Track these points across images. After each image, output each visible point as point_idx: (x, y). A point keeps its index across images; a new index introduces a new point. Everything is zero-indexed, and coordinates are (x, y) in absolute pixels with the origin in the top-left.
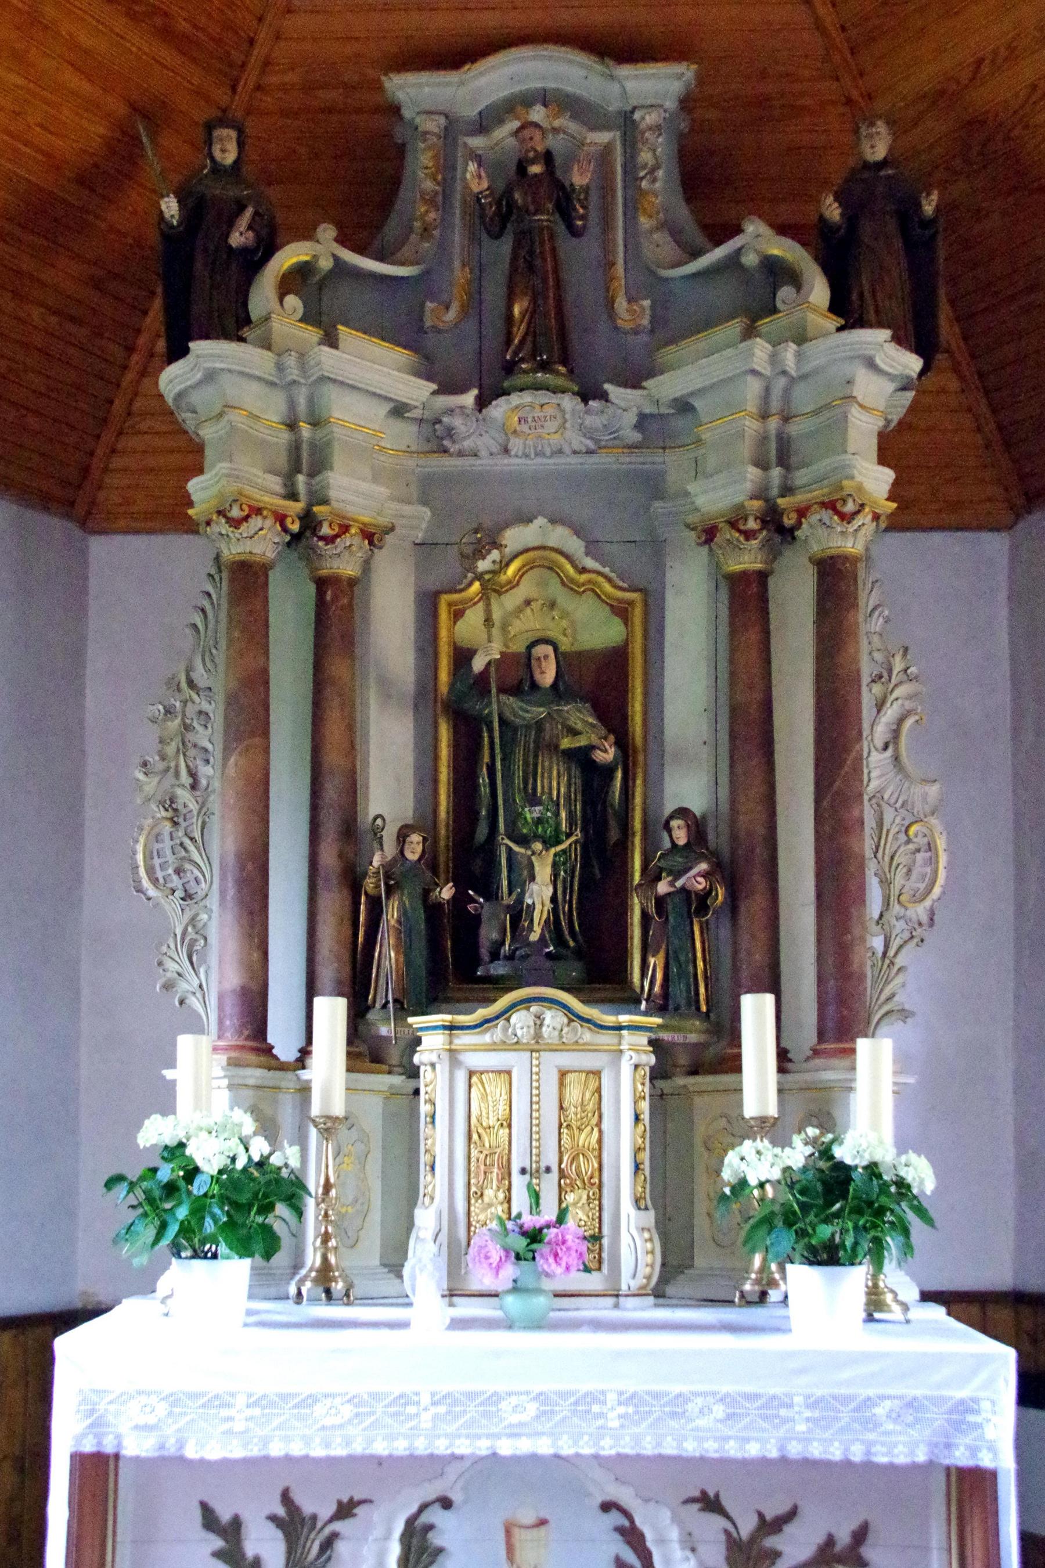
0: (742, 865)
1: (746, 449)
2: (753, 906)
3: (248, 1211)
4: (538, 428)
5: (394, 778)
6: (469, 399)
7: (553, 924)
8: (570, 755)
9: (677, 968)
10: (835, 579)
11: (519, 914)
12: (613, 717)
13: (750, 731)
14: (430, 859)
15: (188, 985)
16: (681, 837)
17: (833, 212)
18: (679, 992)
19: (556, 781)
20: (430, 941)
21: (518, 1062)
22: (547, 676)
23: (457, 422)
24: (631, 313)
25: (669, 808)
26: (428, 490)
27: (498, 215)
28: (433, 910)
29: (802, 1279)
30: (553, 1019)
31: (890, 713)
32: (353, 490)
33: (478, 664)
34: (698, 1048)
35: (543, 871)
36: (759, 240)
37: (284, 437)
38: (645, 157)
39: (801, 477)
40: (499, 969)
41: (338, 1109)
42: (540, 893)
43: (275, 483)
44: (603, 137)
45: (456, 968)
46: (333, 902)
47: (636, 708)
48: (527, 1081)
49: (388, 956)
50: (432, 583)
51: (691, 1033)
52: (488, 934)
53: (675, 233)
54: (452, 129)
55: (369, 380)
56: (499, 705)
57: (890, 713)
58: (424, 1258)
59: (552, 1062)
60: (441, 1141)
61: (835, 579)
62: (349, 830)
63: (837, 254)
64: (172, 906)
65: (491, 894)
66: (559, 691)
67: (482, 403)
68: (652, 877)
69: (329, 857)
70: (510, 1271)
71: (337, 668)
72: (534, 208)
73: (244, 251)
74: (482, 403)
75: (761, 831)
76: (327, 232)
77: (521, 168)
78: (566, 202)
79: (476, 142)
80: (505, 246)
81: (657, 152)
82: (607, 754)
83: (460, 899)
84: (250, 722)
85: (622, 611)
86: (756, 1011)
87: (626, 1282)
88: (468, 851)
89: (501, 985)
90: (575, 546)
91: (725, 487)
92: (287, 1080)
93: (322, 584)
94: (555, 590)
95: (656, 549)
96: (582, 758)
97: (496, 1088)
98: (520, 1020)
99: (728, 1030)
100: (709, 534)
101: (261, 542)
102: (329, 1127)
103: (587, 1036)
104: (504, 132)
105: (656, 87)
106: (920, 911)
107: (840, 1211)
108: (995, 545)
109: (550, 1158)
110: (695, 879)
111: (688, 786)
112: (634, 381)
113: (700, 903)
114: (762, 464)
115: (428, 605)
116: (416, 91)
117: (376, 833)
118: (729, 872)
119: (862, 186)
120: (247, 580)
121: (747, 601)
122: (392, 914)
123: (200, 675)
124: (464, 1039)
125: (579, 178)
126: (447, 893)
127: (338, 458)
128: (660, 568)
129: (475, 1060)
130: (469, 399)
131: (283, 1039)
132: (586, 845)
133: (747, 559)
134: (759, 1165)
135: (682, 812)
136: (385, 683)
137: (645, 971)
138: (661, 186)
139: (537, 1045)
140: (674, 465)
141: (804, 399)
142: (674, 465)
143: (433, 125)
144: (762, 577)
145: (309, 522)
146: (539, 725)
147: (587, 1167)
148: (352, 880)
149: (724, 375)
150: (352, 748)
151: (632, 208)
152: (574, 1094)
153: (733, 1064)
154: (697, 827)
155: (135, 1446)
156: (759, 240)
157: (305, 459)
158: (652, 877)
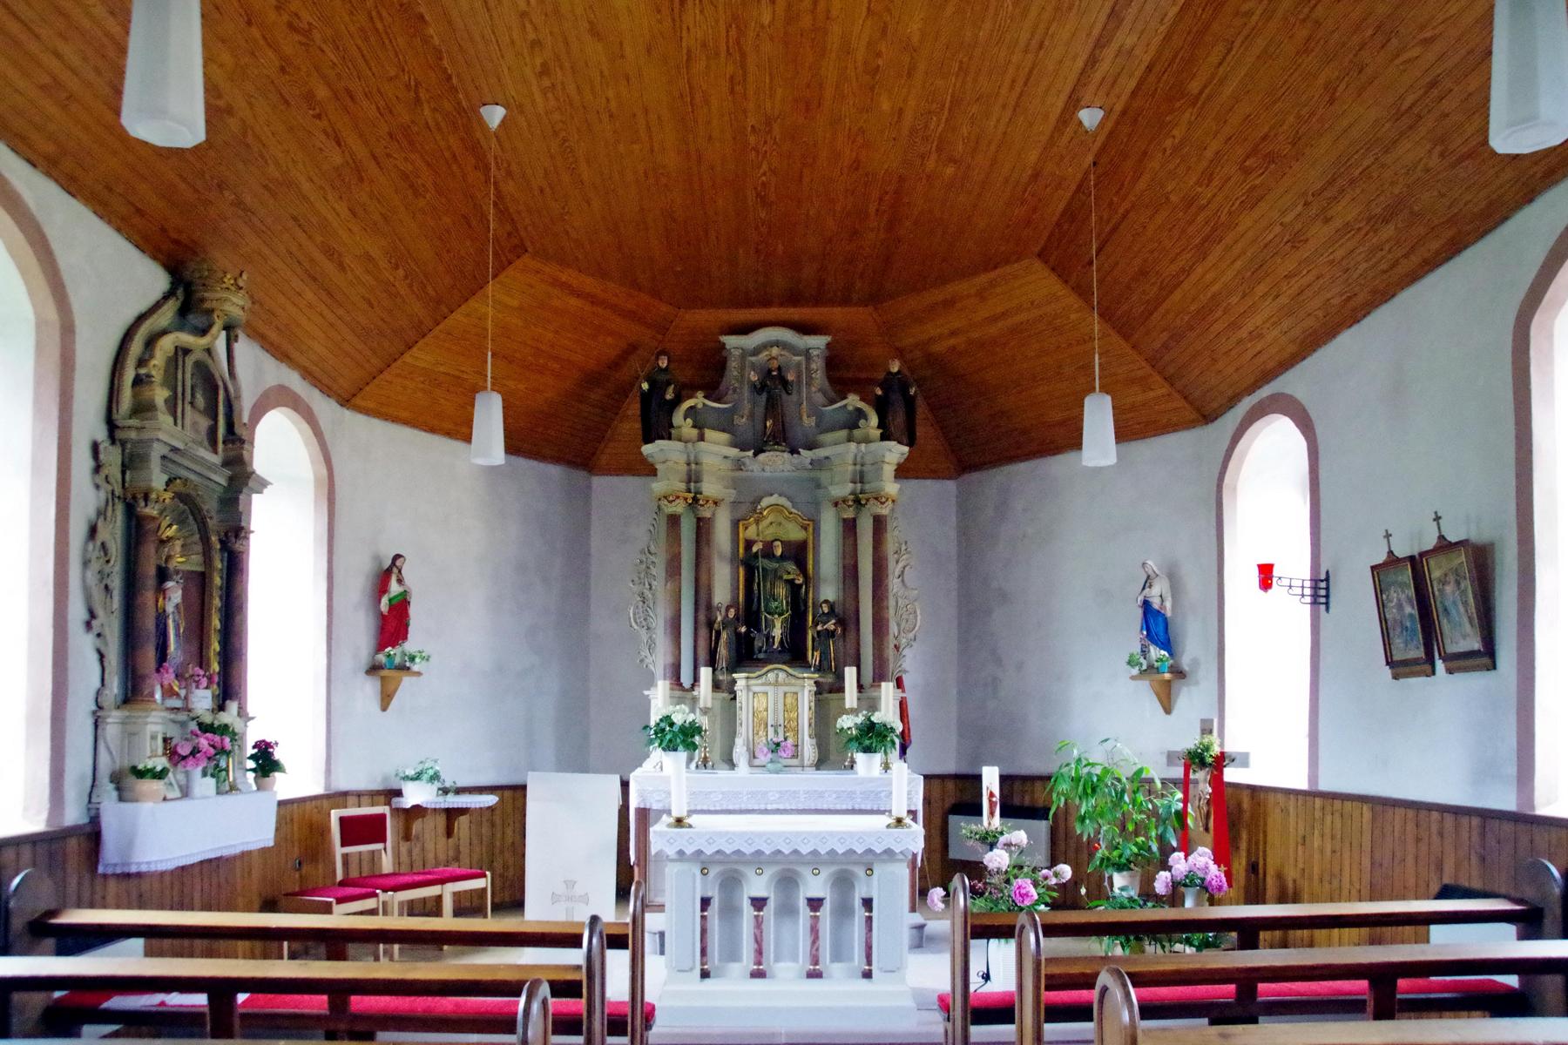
0: (847, 619)
1: (849, 477)
2: (851, 636)
3: (682, 737)
4: (776, 462)
5: (723, 591)
6: (751, 453)
7: (781, 642)
8: (787, 581)
9: (824, 655)
10: (879, 524)
11: (769, 638)
12: (802, 566)
13: (850, 574)
14: (737, 617)
15: (649, 660)
16: (826, 610)
17: (879, 392)
18: (825, 664)
19: (782, 591)
20: (739, 646)
21: (770, 690)
22: (778, 552)
23: (747, 461)
24: (809, 422)
25: (822, 599)
26: (735, 484)
27: (759, 389)
28: (738, 635)
29: (860, 757)
30: (782, 675)
31: (901, 565)
32: (710, 488)
33: (755, 549)
34: (831, 684)
35: (778, 624)
36: (853, 401)
37: (685, 468)
38: (814, 366)
39: (867, 487)
40: (761, 656)
41: (709, 705)
42: (777, 632)
43: (683, 486)
44: (797, 358)
45: (746, 656)
46: (703, 632)
47: (810, 562)
48: (773, 696)
49: (723, 651)
50: (738, 516)
51: (829, 679)
52: (758, 644)
53: (825, 394)
54: (745, 353)
55: (716, 450)
56: (762, 562)
57: (901, 565)
58: (740, 753)
59: (782, 689)
60: (744, 715)
61: (879, 524)
62: (709, 607)
63: (882, 407)
64: (644, 631)
65: (759, 630)
66: (783, 557)
67: (755, 455)
68: (815, 624)
69: (702, 617)
70: (770, 755)
71: (705, 550)
72: (773, 385)
73: (671, 401)
74: (755, 455)
75: (853, 608)
76: (700, 394)
77: (770, 371)
78: (785, 383)
79: (753, 359)
80: (764, 396)
81: (818, 365)
82: (800, 581)
83: (748, 632)
84: (674, 569)
85: (805, 528)
86: (850, 673)
87: (806, 762)
88: (750, 613)
89: (765, 662)
90: (788, 504)
91: (843, 490)
92: (689, 695)
93: (699, 520)
94: (781, 519)
95: (816, 504)
96: (791, 582)
97: (763, 699)
98: (771, 676)
99: (840, 677)
100: (836, 504)
101: (679, 508)
102: (705, 711)
103: (793, 681)
104: (763, 356)
105: (818, 342)
106: (911, 635)
107: (872, 736)
108: (950, 485)
109: (781, 721)
110: (831, 625)
111: (829, 592)
112: (810, 449)
113: (831, 634)
114: (854, 482)
115: (735, 524)
116: (731, 341)
117: (719, 609)
118: (841, 622)
119: (889, 382)
120: (674, 520)
121: (850, 527)
122: (724, 635)
123: (652, 548)
124: (752, 682)
125: (790, 377)
126: (743, 629)
127: (705, 478)
128: (818, 512)
129: (756, 689)
130: (751, 453)
131: (686, 679)
132: (792, 616)
133: (849, 514)
134: (847, 722)
135: (826, 601)
136: (720, 554)
137: (813, 657)
138: (819, 377)
139: (776, 684)
140: (824, 476)
141: (868, 459)
142: (824, 476)
143: (737, 353)
144: (854, 520)
145: (695, 500)
146: (776, 570)
147: (793, 724)
148: (710, 624)
149: (841, 452)
150: (710, 579)
151: (809, 384)
152: (789, 700)
153: (841, 689)
154: (832, 606)
155: (655, 807)
156: (853, 401)
157: (693, 478)
158: (815, 624)
